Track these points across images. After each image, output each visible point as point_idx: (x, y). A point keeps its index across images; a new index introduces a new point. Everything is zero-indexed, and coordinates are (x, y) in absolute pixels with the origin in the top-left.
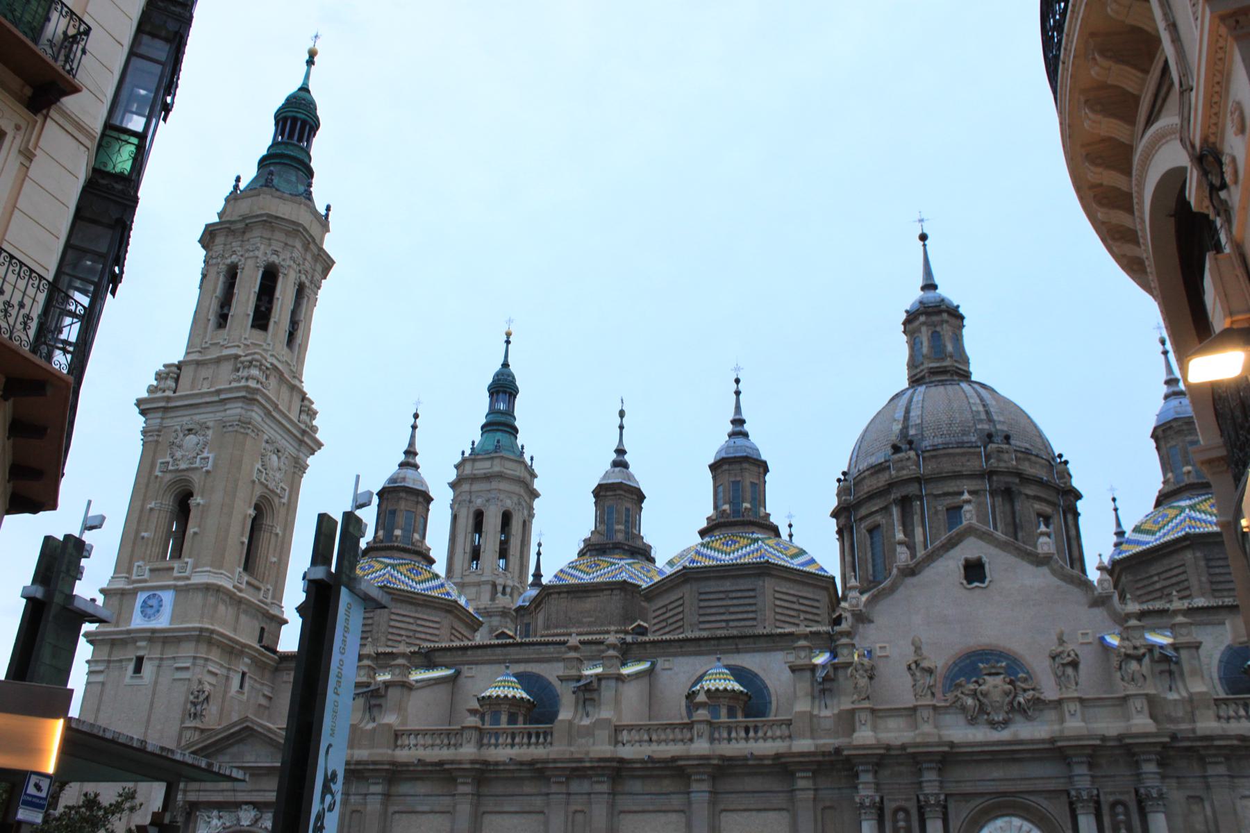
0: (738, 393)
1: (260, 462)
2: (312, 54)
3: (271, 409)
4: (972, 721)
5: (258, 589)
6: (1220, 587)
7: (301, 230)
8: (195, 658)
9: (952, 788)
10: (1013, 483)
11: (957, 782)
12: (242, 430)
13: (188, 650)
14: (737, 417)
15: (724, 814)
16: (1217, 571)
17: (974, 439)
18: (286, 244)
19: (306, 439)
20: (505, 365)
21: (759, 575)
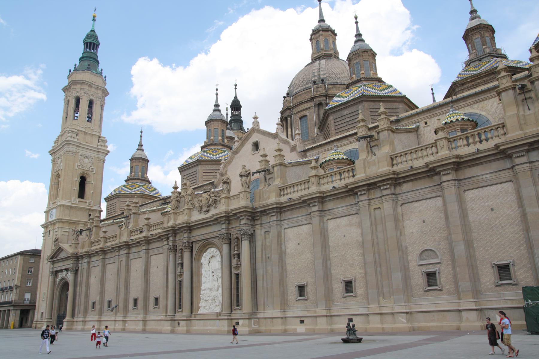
0: (217, 94)
1: (79, 163)
2: (94, 17)
3: (78, 145)
4: (200, 211)
5: (86, 202)
6: (339, 130)
7: (84, 82)
8: (58, 228)
9: (192, 240)
10: (322, 100)
11: (194, 237)
12: (68, 154)
13: (57, 225)
14: (217, 104)
15: (152, 256)
16: (338, 123)
17: (309, 85)
18: (81, 88)
19: (99, 150)
20: (236, 97)
21: (197, 165)
